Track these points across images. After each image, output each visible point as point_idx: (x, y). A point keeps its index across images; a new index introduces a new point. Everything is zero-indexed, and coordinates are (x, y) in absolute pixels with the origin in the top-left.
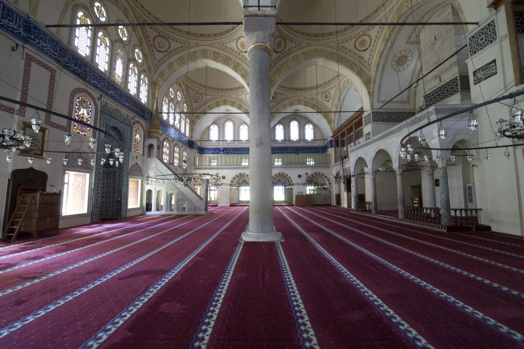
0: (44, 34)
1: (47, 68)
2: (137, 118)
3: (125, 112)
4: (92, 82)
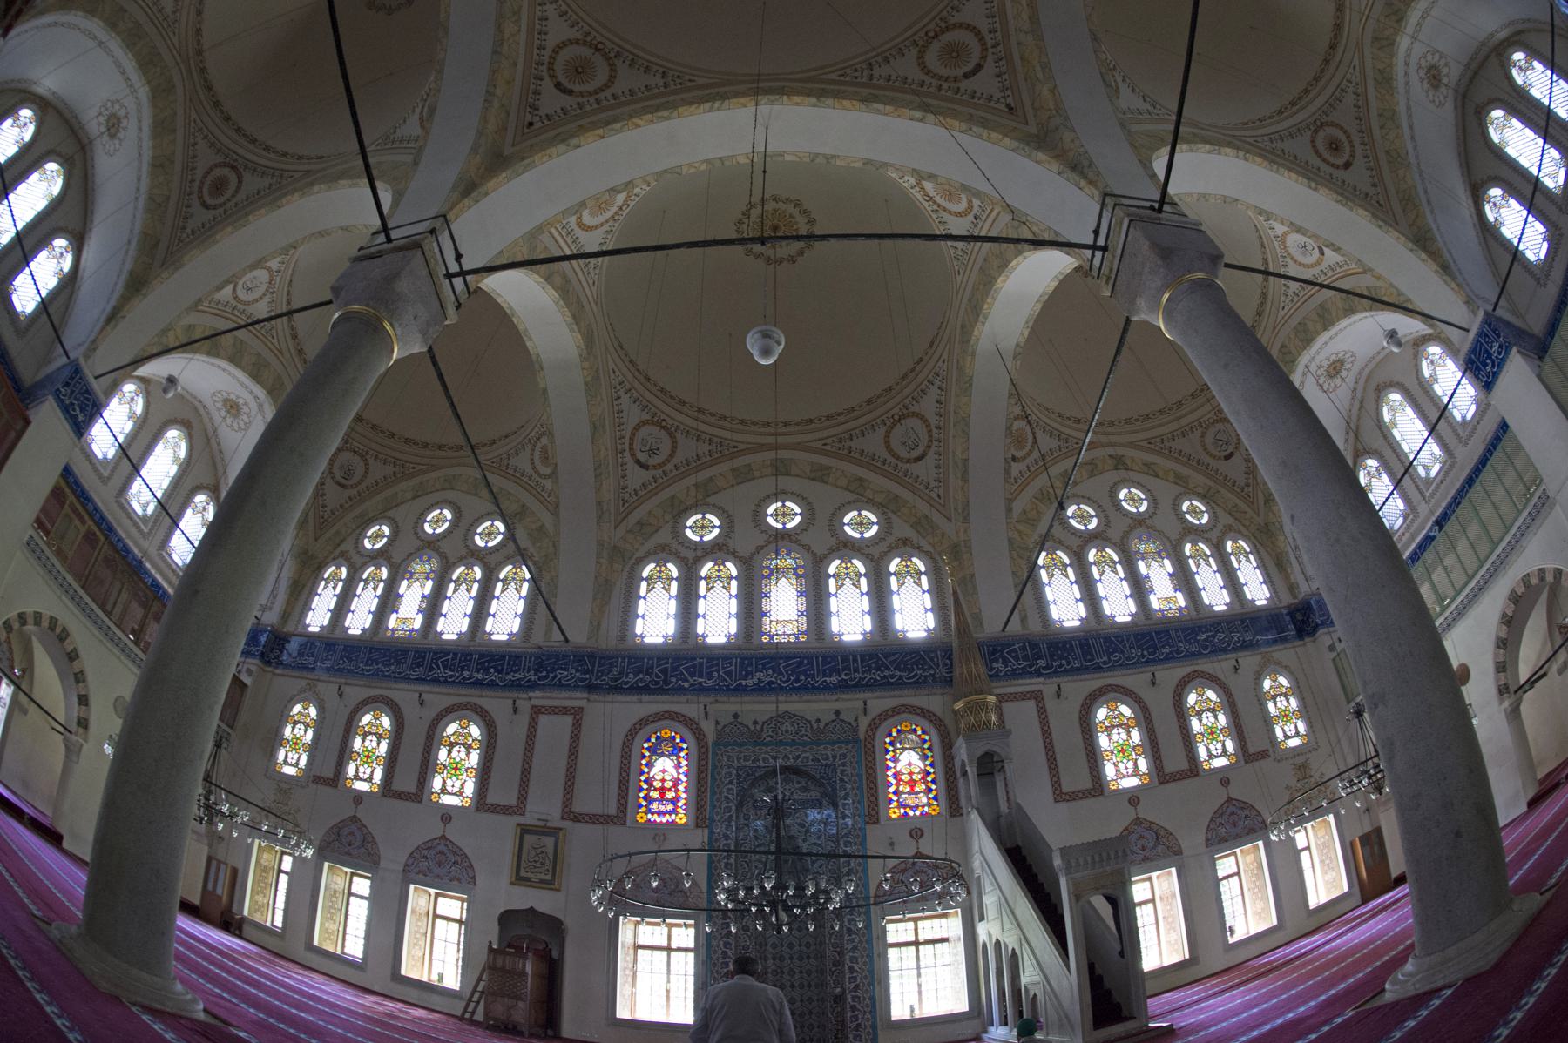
0: (566, 656)
1: (564, 711)
2: (879, 702)
3: (817, 708)
4: (686, 685)
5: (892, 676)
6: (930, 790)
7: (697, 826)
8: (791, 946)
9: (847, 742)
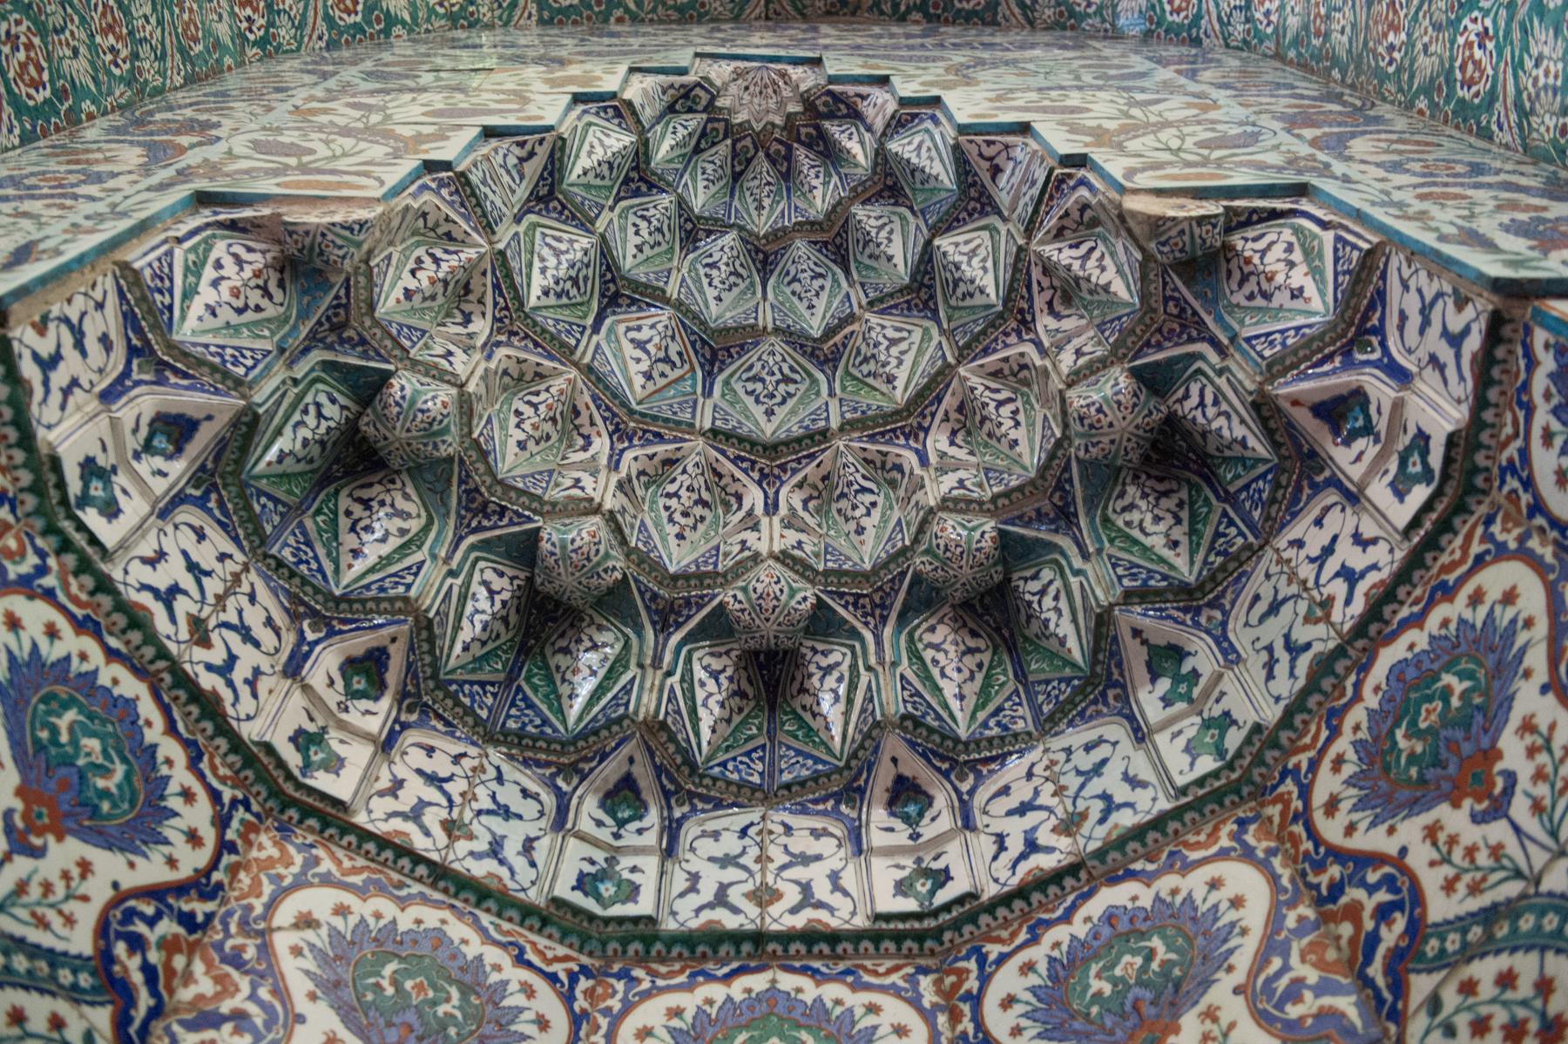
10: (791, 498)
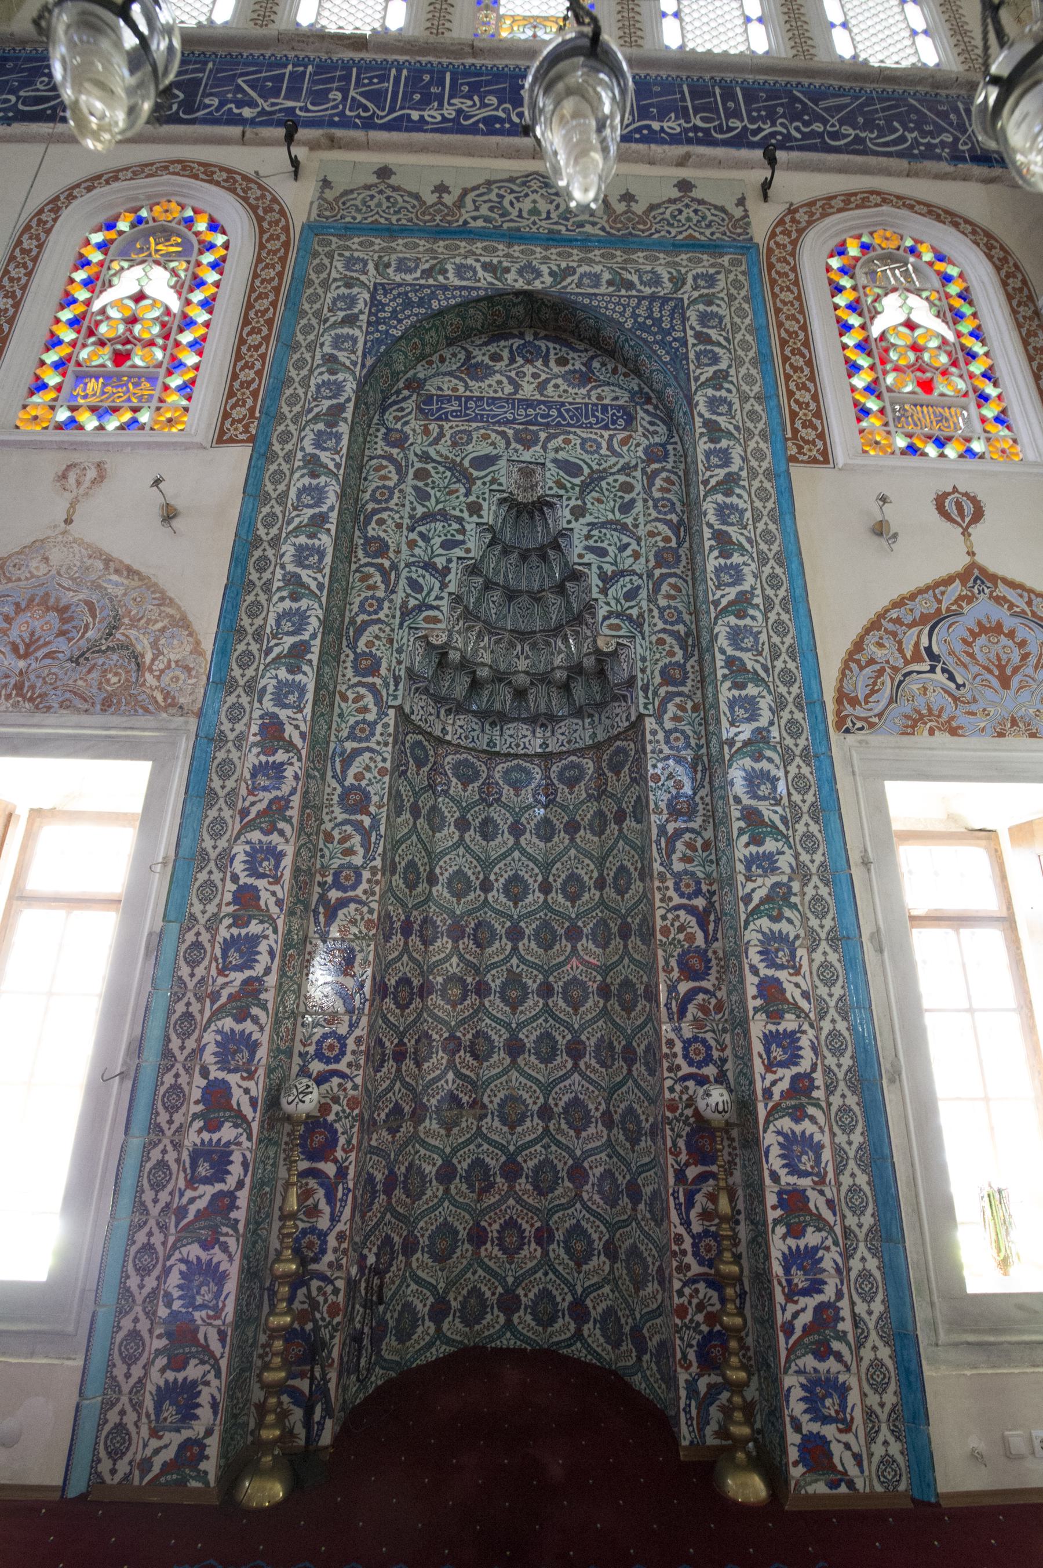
5: (835, 136)
6: (984, 398)
7: (222, 438)
8: (516, 888)
9: (713, 248)
10: (527, 648)
